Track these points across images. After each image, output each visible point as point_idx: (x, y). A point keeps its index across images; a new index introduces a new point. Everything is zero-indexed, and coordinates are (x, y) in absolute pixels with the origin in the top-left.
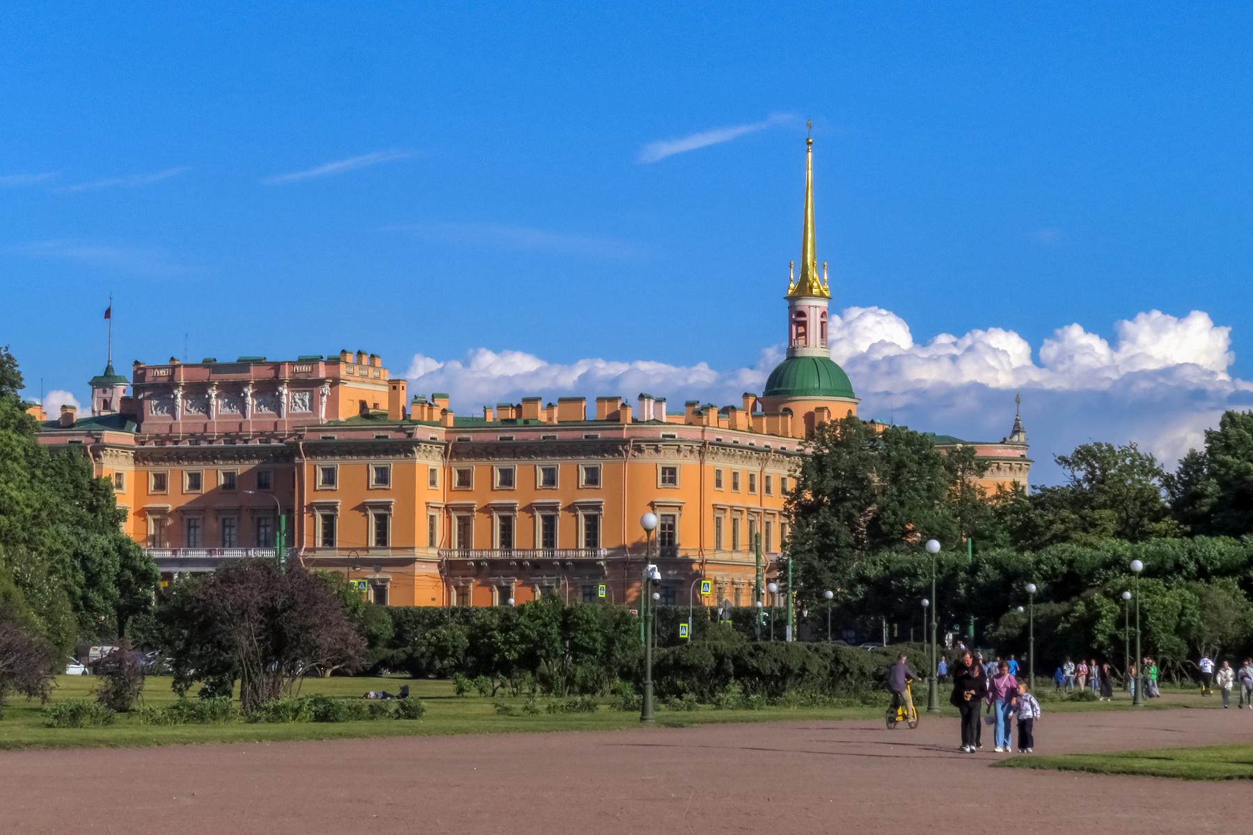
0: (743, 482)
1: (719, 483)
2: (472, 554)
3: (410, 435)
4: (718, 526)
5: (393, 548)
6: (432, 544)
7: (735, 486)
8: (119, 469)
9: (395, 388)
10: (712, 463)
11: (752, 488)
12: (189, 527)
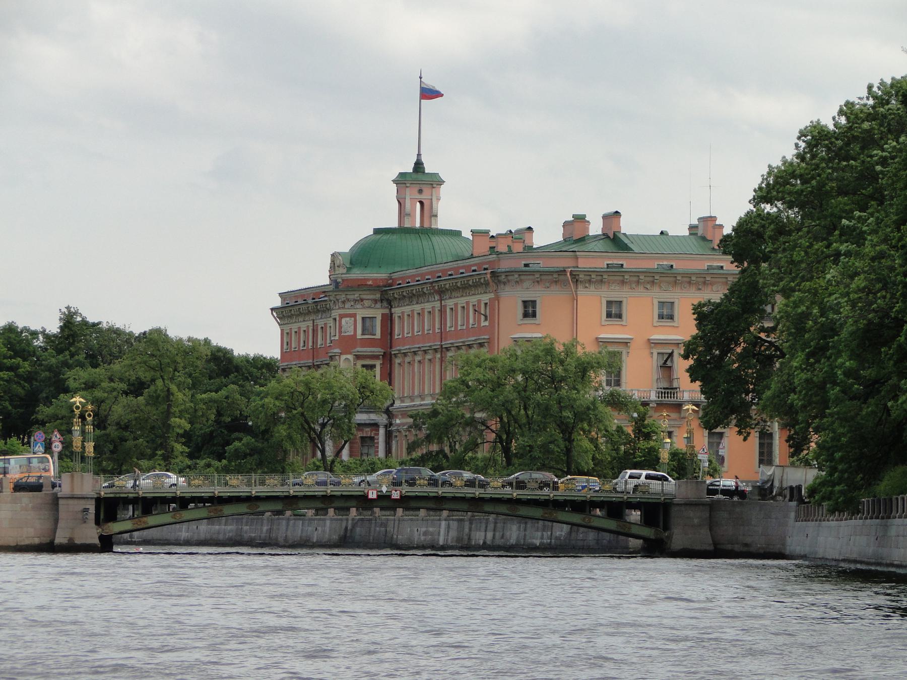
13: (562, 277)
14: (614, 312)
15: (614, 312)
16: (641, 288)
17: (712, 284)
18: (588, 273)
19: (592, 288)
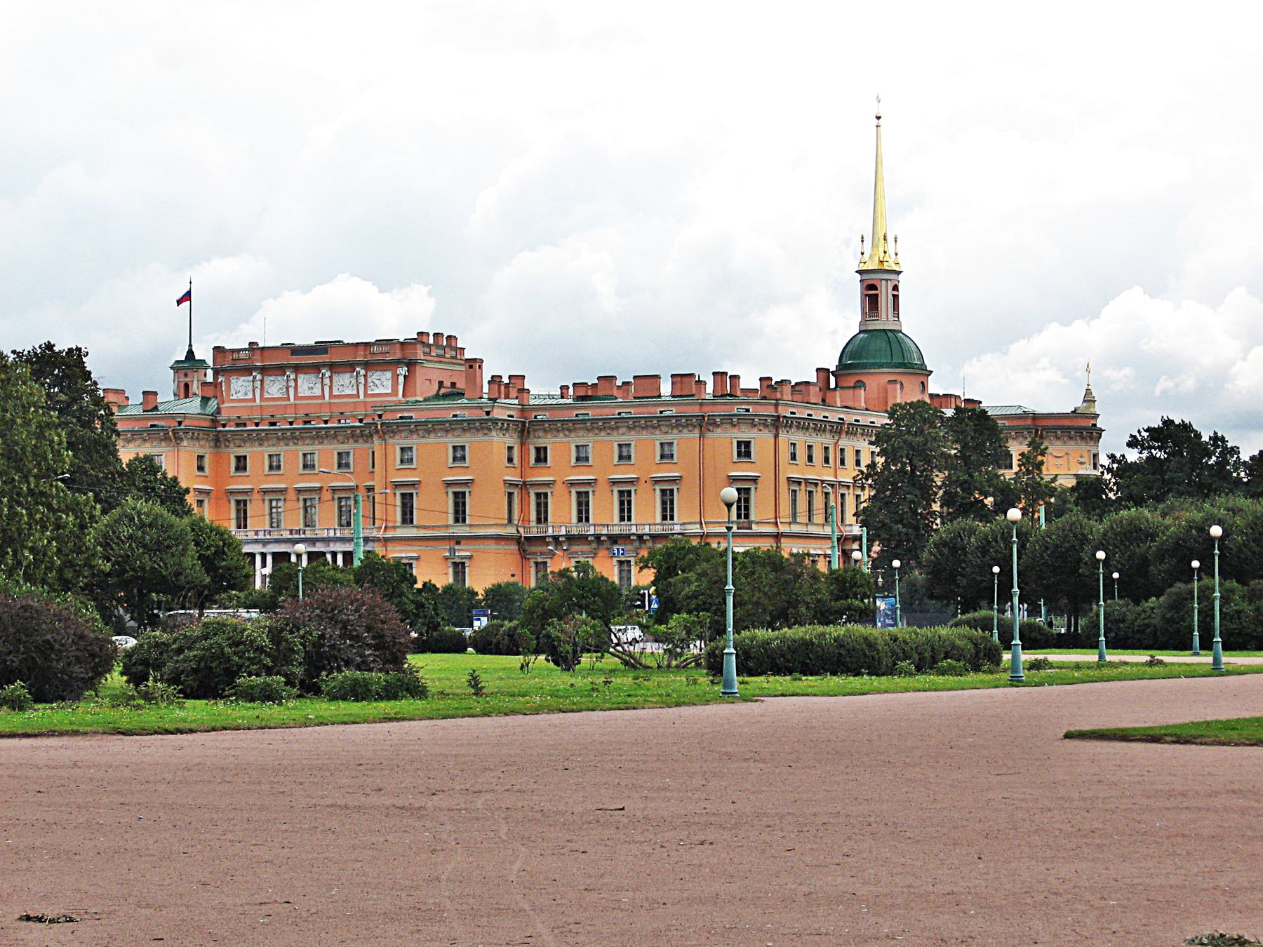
0: (818, 455)
1: (793, 457)
2: (550, 530)
3: (488, 413)
4: (794, 501)
5: (470, 526)
6: (510, 520)
7: (810, 459)
8: (201, 452)
9: (471, 367)
10: (784, 437)
11: (827, 460)
12: (271, 508)
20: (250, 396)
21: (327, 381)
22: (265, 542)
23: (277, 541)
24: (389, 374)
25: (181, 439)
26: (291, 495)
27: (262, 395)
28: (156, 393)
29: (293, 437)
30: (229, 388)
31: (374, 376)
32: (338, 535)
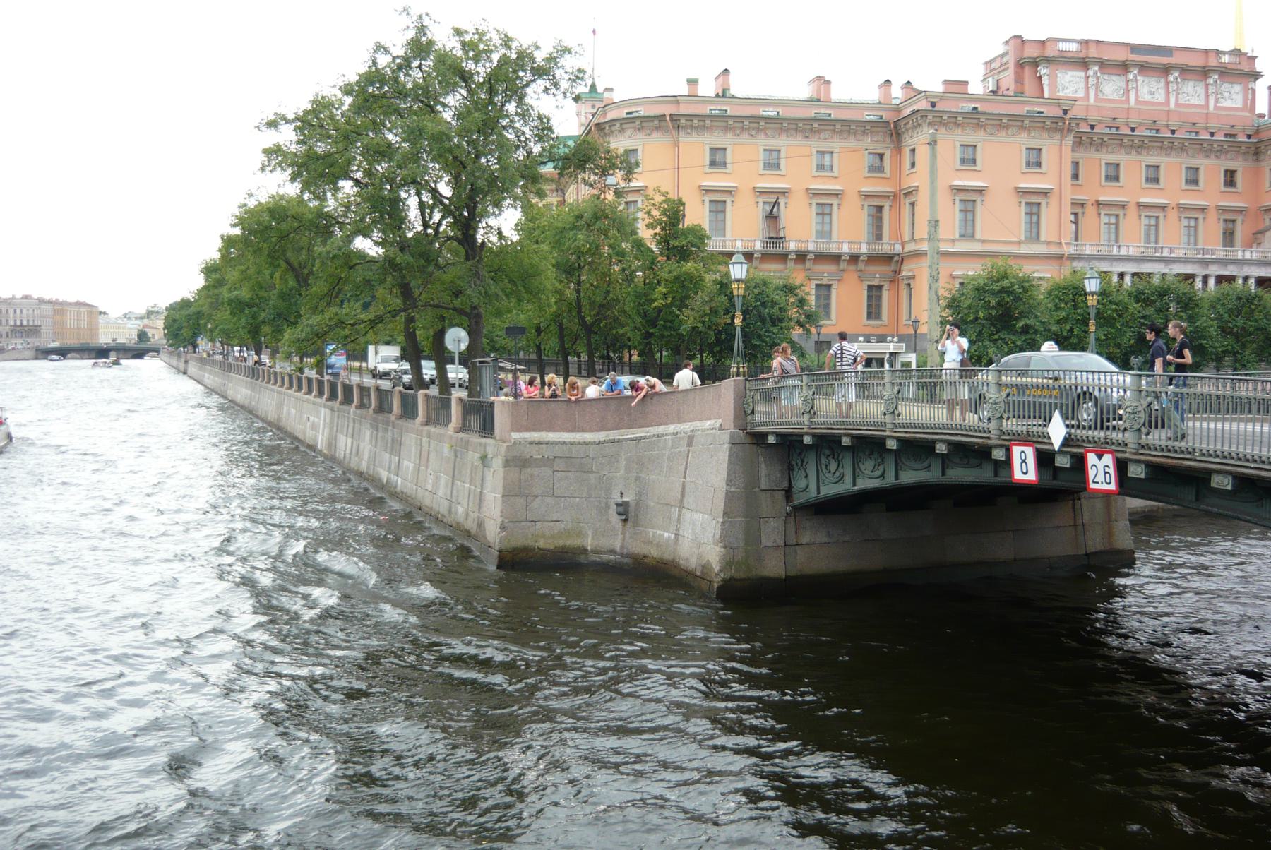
13: (663, 124)
14: (717, 160)
15: (717, 160)
16: (745, 135)
17: (819, 132)
18: (690, 117)
19: (695, 134)
20: (1081, 94)
21: (1173, 87)
22: (1168, 261)
23: (1185, 261)
24: (1237, 88)
25: (1069, 130)
26: (1132, 210)
27: (1096, 95)
28: (966, 83)
29: (1137, 144)
30: (1053, 85)
31: (1226, 86)
32: (1254, 257)
